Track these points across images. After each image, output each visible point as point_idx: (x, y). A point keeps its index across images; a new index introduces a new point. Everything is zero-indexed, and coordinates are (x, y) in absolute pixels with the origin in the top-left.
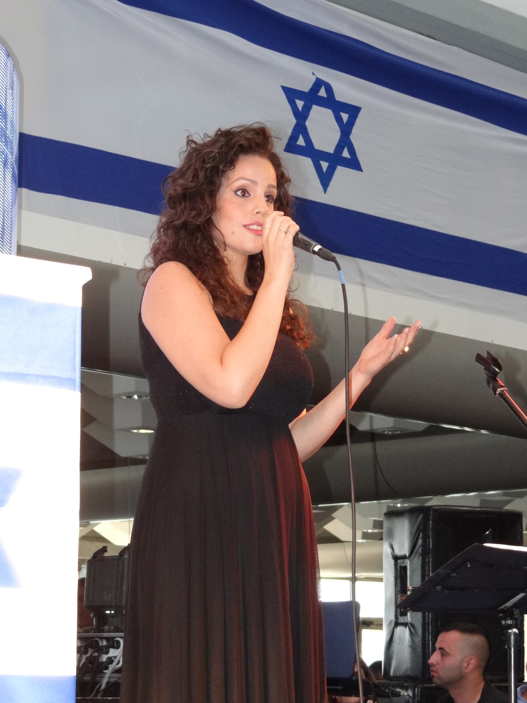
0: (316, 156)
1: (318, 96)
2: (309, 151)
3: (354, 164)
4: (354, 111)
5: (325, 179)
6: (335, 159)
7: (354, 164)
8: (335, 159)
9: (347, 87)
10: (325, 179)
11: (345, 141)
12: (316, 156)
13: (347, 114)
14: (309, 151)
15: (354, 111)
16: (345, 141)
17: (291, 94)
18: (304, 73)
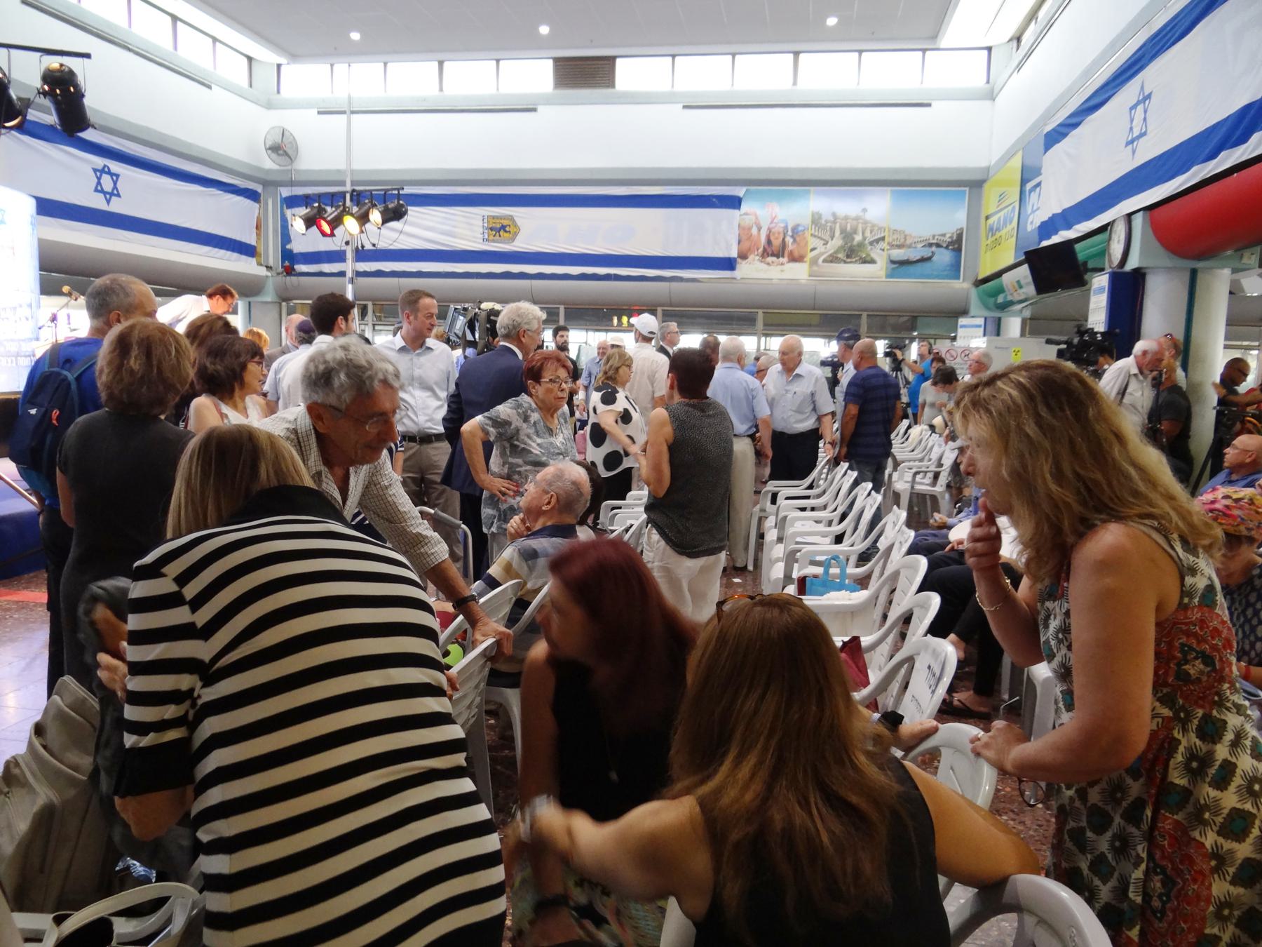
0: (105, 193)
1: (104, 171)
2: (102, 191)
3: (118, 195)
4: (118, 176)
5: (108, 202)
6: (112, 194)
7: (118, 195)
8: (112, 194)
9: (115, 166)
10: (108, 202)
11: (115, 187)
12: (105, 193)
13: (115, 177)
14: (102, 191)
15: (118, 176)
16: (115, 187)
17: (95, 170)
18: (99, 162)
